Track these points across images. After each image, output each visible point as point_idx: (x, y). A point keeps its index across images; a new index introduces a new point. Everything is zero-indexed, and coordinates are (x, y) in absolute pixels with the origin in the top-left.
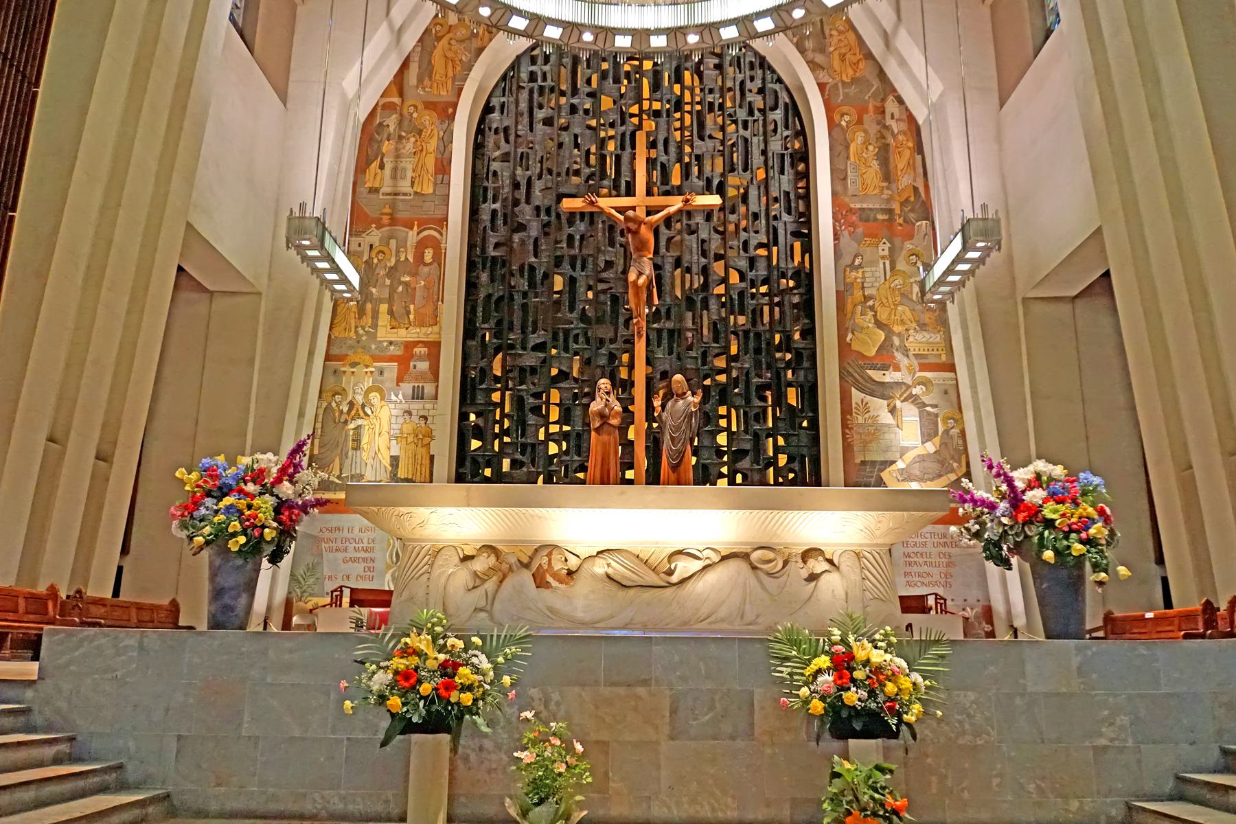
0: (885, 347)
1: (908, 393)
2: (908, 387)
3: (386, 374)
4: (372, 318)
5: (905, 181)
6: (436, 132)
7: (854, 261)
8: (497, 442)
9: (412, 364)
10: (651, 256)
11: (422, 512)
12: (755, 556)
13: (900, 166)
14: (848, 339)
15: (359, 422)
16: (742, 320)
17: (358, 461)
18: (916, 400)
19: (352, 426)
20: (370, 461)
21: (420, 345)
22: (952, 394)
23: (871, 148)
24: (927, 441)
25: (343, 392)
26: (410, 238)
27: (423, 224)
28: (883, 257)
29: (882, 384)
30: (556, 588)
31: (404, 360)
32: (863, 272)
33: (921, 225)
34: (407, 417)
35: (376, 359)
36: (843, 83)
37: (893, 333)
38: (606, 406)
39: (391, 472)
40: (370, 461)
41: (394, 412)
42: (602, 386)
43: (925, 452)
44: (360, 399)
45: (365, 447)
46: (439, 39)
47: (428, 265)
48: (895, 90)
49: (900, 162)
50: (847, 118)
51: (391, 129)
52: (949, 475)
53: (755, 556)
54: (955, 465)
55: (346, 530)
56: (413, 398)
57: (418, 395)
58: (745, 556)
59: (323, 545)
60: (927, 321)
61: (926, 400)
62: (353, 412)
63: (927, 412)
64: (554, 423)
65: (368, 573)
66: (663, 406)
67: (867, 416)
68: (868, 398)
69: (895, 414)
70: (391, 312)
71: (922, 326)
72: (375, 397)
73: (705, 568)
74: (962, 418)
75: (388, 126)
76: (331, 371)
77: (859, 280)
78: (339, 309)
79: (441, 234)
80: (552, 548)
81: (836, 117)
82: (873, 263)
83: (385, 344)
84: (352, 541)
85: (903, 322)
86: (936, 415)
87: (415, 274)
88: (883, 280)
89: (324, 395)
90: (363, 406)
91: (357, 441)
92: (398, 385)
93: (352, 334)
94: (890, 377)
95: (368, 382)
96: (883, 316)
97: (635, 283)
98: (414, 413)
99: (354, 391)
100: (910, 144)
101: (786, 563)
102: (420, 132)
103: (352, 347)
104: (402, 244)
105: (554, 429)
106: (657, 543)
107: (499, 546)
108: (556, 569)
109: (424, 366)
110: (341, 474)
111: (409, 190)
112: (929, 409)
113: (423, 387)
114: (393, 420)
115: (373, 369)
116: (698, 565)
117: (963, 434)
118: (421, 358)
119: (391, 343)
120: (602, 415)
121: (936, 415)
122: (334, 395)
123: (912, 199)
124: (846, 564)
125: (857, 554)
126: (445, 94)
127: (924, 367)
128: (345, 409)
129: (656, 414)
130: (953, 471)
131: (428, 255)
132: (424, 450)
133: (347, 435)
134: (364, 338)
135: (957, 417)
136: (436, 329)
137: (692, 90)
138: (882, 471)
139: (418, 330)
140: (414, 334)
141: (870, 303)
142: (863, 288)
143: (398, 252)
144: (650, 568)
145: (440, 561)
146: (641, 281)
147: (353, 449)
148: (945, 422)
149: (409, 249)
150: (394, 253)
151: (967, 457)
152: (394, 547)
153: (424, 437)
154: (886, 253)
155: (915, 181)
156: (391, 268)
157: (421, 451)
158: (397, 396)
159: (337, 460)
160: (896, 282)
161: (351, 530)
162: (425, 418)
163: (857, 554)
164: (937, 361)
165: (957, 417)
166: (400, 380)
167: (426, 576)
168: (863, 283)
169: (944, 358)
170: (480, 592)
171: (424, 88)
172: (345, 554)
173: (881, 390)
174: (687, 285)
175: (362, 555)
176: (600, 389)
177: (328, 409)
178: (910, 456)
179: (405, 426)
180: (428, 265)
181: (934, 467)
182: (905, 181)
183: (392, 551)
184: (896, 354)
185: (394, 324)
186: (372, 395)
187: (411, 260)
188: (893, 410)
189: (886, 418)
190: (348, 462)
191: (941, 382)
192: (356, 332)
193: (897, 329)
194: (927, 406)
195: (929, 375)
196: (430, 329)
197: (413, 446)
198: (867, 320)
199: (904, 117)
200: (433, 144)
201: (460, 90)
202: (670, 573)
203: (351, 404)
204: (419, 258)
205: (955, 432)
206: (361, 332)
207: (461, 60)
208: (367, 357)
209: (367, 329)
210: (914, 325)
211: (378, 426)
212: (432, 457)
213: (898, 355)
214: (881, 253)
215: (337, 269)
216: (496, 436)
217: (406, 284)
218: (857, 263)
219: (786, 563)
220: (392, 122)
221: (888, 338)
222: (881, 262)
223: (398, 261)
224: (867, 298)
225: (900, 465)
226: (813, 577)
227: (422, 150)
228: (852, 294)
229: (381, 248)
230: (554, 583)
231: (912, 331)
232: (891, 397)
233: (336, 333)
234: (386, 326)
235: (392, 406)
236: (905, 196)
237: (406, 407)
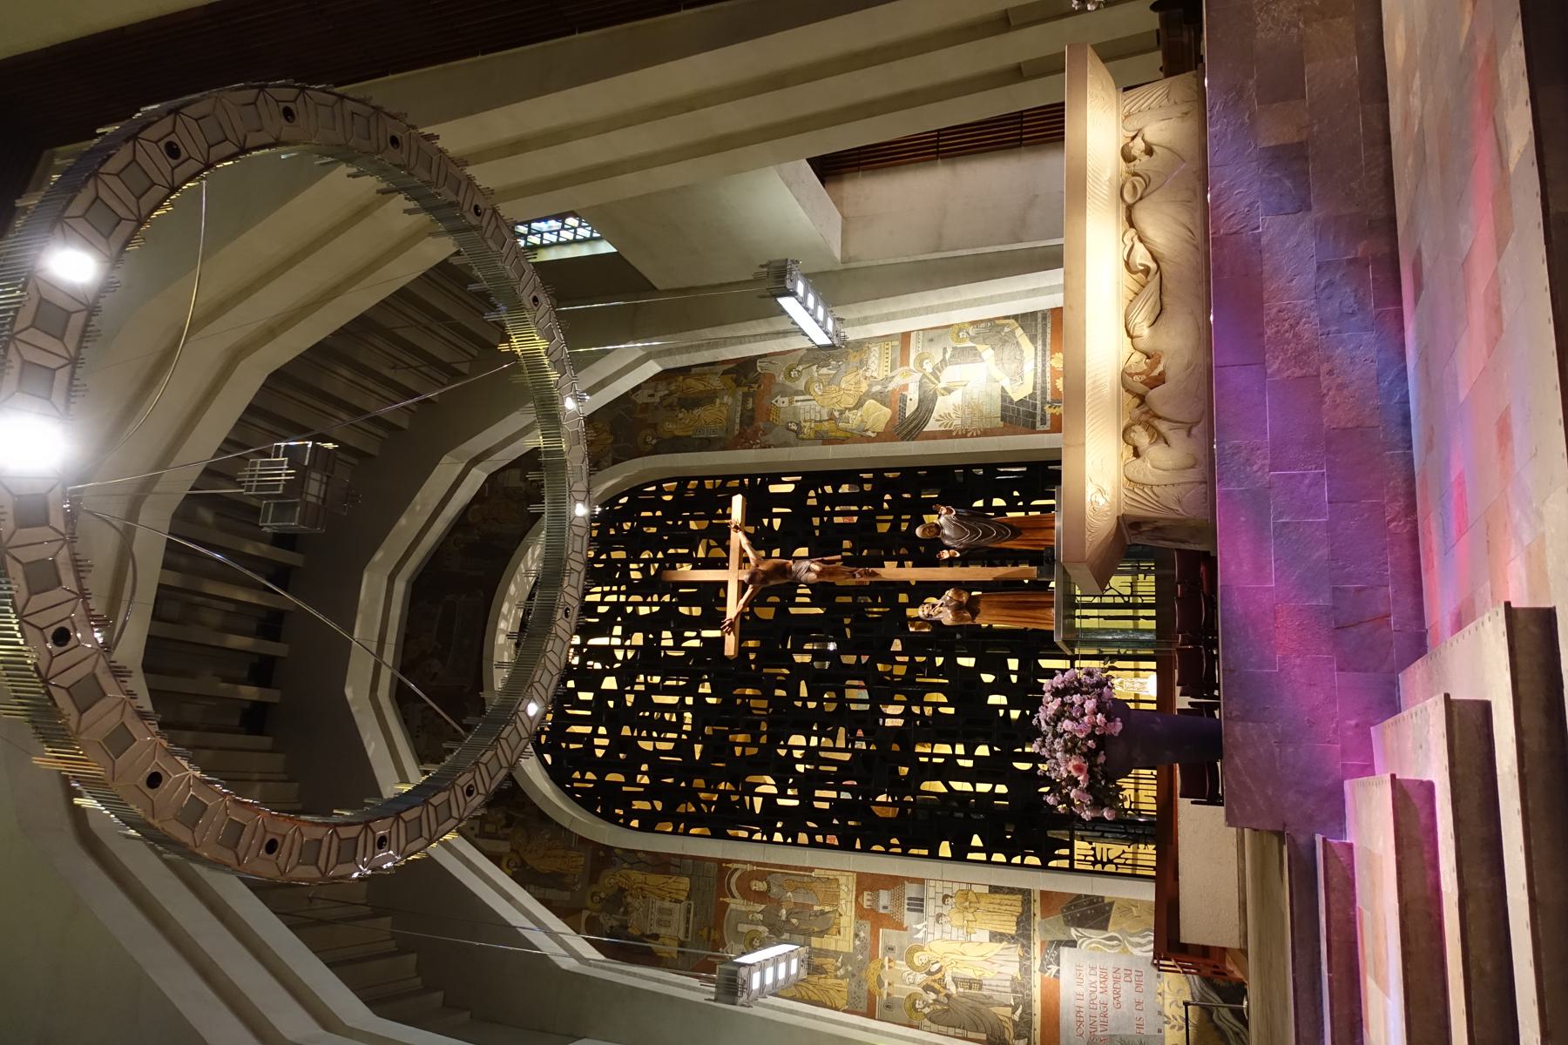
0: (882, 398)
1: (930, 376)
2: (924, 376)
3: (893, 943)
4: (826, 957)
5: (716, 382)
6: (624, 871)
7: (793, 430)
8: (975, 817)
9: (882, 911)
10: (791, 562)
11: (1091, 493)
12: (1128, 198)
13: (702, 388)
14: (873, 435)
15: (948, 979)
16: (847, 544)
17: (994, 983)
18: (938, 369)
19: (952, 989)
20: (996, 968)
21: (860, 900)
22: (932, 335)
23: (680, 415)
24: (980, 356)
25: (912, 998)
26: (739, 908)
27: (724, 890)
28: (791, 402)
29: (920, 401)
30: (1164, 367)
32: (805, 421)
33: (761, 367)
34: (944, 919)
35: (874, 956)
36: (614, 442)
37: (868, 391)
38: (947, 606)
39: (1009, 943)
40: (996, 968)
41: (937, 935)
42: (926, 613)
43: (993, 359)
44: (921, 978)
45: (978, 973)
46: (523, 863)
47: (769, 887)
48: (627, 393)
49: (696, 386)
50: (649, 439)
51: (615, 923)
52: (1017, 335)
53: (1128, 198)
54: (1006, 330)
55: (1080, 1003)
56: (922, 911)
57: (918, 905)
58: (1130, 209)
59: (1098, 1033)
60: (857, 359)
61: (938, 358)
62: (937, 986)
63: (953, 356)
64: (953, 749)
65: (1133, 977)
66: (948, 548)
67: (953, 416)
68: (935, 414)
69: (952, 388)
70: (821, 934)
71: (862, 364)
72: (919, 958)
73: (1141, 240)
74: (958, 324)
75: (611, 927)
76: (886, 1011)
77: (813, 425)
78: (815, 998)
79: (736, 869)
80: (1125, 376)
81: (649, 448)
82: (795, 412)
83: (857, 943)
84: (1093, 996)
85: (859, 382)
86: (955, 349)
87: (779, 904)
88: (814, 402)
89: (915, 1023)
90: (930, 973)
91: (970, 983)
92: (906, 929)
93: (844, 983)
94: (913, 396)
95: (902, 965)
96: (851, 402)
97: (819, 574)
98: (939, 910)
99: (911, 984)
100: (681, 378)
101: (1135, 174)
102: (622, 890)
103: (859, 984)
104: (744, 917)
105: (960, 749)
106: (1118, 283)
107: (1124, 424)
108: (1145, 367)
109: (884, 897)
110: (1010, 1006)
111: (684, 905)
112: (948, 356)
113: (909, 899)
114: (947, 936)
115: (887, 959)
116: (1139, 247)
117: (973, 323)
118: (876, 900)
119: (856, 935)
120: (958, 609)
121: (955, 349)
122: (916, 1010)
123: (735, 376)
124: (1135, 124)
125: (1126, 117)
126: (580, 860)
127: (905, 360)
128: (933, 996)
129: (958, 555)
130: (1013, 332)
131: (760, 886)
132: (983, 901)
133: (964, 996)
134: (850, 969)
135: (956, 329)
136: (842, 880)
137: (604, 594)
138: (1012, 400)
139: (843, 901)
140: (847, 908)
141: (836, 414)
142: (821, 421)
143: (751, 922)
144: (1141, 290)
145: (1140, 478)
146: (816, 567)
147: (980, 989)
148: (963, 340)
149: (750, 908)
150: (754, 927)
151: (999, 318)
152: (1099, 943)
153: (967, 901)
154: (786, 400)
155: (716, 373)
156: (771, 931)
157: (983, 904)
158: (918, 931)
159: (994, 1009)
160: (816, 390)
161: (1079, 996)
162: (945, 897)
163: (1126, 117)
164: (899, 348)
165: (956, 329)
166: (899, 926)
167: (1155, 488)
168: (816, 421)
169: (896, 343)
170: (1171, 435)
171: (575, 884)
172: (1110, 1005)
173: (926, 405)
174: (807, 600)
175: (1110, 983)
176: (929, 615)
177: (932, 1018)
178: (998, 374)
179: (954, 922)
180: (769, 887)
181: (1008, 351)
182: (716, 382)
183: (1104, 945)
184: (890, 389)
185: (834, 930)
186: (917, 962)
187: (763, 906)
188: (948, 391)
190: (996, 996)
191: (920, 345)
192: (842, 978)
193: (864, 387)
194: (944, 358)
195: (913, 356)
196: (843, 887)
197: (979, 914)
198: (854, 419)
199: (653, 384)
200: (637, 876)
202: (1147, 271)
203: (927, 988)
204: (762, 896)
205: (972, 331)
206: (841, 972)
207: (550, 840)
208: (872, 966)
209: (839, 964)
210: (861, 371)
211: (954, 956)
212: (994, 890)
214: (786, 404)
215: (775, 961)
216: (967, 816)
217: (788, 915)
218: (795, 428)
219: (1135, 174)
220: (608, 921)
221: (874, 396)
222: (795, 404)
223: (763, 923)
224: (831, 418)
226: (1149, 151)
227: (641, 888)
228: (827, 432)
229: (747, 942)
230: (1160, 368)
231: (867, 374)
232: (935, 393)
233: (841, 1003)
234: (837, 941)
235: (930, 937)
236: (730, 382)
237: (931, 920)
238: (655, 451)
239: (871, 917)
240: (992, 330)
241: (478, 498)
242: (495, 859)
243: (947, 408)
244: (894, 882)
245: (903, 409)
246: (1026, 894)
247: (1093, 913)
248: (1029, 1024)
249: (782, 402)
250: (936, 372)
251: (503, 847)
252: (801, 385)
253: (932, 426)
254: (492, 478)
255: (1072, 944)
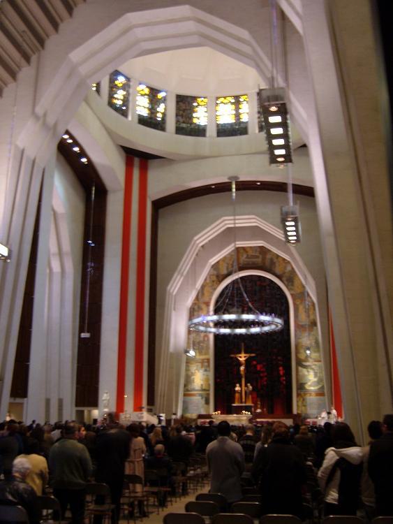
31: (202, 362)
44: (193, 371)
57: (206, 370)
71: (315, 352)
72: (197, 371)
109: (206, 364)
126: (206, 299)
127: (315, 361)
131: (206, 339)
153: (207, 380)
166: (202, 367)
178: (311, 381)
182: (312, 317)
188: (308, 371)
189: (306, 373)
201: (210, 299)
213: (309, 359)
220: (196, 307)
225: (309, 383)
238: (295, 304)
239: (202, 362)
240: (320, 381)
241: (284, 259)
242: (206, 280)
243: (304, 371)
244: (209, 366)
245: (305, 361)
246: (208, 390)
247: (207, 402)
248: (189, 391)
249: (306, 334)
250: (313, 369)
251: (208, 281)
252: (311, 338)
253: (300, 368)
254: (289, 262)
255: (202, 398)
